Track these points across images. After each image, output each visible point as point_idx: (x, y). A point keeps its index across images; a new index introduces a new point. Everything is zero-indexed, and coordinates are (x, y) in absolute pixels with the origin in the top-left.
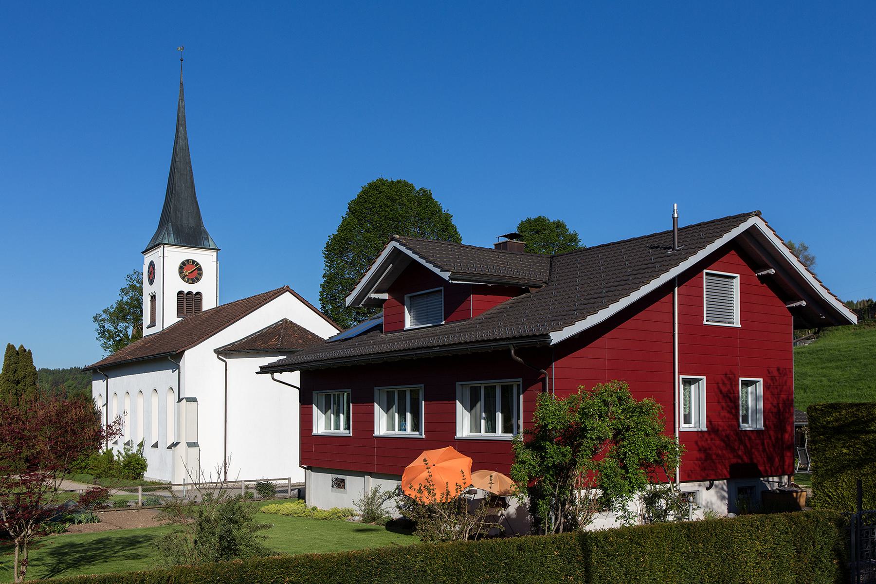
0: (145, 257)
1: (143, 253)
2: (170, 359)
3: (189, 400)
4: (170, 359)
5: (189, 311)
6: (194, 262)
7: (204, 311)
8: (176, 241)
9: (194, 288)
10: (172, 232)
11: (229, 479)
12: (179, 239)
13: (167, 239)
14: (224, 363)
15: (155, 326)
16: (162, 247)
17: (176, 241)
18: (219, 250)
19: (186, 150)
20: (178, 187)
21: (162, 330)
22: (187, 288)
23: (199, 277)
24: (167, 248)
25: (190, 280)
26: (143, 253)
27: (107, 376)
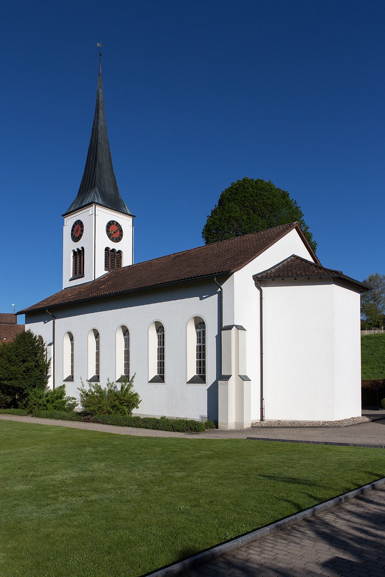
0: (65, 219)
1: (63, 216)
2: (216, 281)
3: (72, 354)
4: (216, 281)
5: (113, 267)
6: (117, 223)
7: (123, 268)
8: (103, 203)
9: (116, 246)
10: (99, 195)
11: (268, 417)
12: (105, 202)
13: (97, 200)
14: (259, 292)
15: (83, 277)
16: (94, 206)
17: (103, 203)
18: (134, 217)
19: (104, 130)
20: (101, 159)
21: (93, 279)
22: (112, 245)
23: (111, 237)
24: (98, 208)
25: (115, 239)
26: (63, 216)
27: (54, 317)
